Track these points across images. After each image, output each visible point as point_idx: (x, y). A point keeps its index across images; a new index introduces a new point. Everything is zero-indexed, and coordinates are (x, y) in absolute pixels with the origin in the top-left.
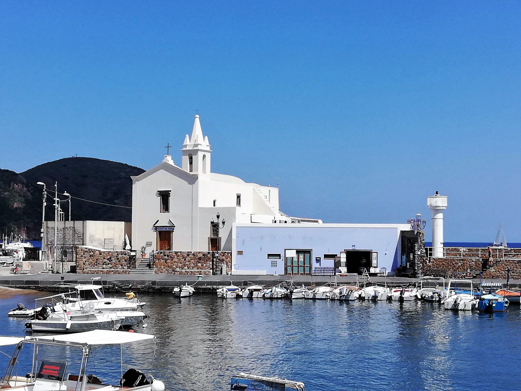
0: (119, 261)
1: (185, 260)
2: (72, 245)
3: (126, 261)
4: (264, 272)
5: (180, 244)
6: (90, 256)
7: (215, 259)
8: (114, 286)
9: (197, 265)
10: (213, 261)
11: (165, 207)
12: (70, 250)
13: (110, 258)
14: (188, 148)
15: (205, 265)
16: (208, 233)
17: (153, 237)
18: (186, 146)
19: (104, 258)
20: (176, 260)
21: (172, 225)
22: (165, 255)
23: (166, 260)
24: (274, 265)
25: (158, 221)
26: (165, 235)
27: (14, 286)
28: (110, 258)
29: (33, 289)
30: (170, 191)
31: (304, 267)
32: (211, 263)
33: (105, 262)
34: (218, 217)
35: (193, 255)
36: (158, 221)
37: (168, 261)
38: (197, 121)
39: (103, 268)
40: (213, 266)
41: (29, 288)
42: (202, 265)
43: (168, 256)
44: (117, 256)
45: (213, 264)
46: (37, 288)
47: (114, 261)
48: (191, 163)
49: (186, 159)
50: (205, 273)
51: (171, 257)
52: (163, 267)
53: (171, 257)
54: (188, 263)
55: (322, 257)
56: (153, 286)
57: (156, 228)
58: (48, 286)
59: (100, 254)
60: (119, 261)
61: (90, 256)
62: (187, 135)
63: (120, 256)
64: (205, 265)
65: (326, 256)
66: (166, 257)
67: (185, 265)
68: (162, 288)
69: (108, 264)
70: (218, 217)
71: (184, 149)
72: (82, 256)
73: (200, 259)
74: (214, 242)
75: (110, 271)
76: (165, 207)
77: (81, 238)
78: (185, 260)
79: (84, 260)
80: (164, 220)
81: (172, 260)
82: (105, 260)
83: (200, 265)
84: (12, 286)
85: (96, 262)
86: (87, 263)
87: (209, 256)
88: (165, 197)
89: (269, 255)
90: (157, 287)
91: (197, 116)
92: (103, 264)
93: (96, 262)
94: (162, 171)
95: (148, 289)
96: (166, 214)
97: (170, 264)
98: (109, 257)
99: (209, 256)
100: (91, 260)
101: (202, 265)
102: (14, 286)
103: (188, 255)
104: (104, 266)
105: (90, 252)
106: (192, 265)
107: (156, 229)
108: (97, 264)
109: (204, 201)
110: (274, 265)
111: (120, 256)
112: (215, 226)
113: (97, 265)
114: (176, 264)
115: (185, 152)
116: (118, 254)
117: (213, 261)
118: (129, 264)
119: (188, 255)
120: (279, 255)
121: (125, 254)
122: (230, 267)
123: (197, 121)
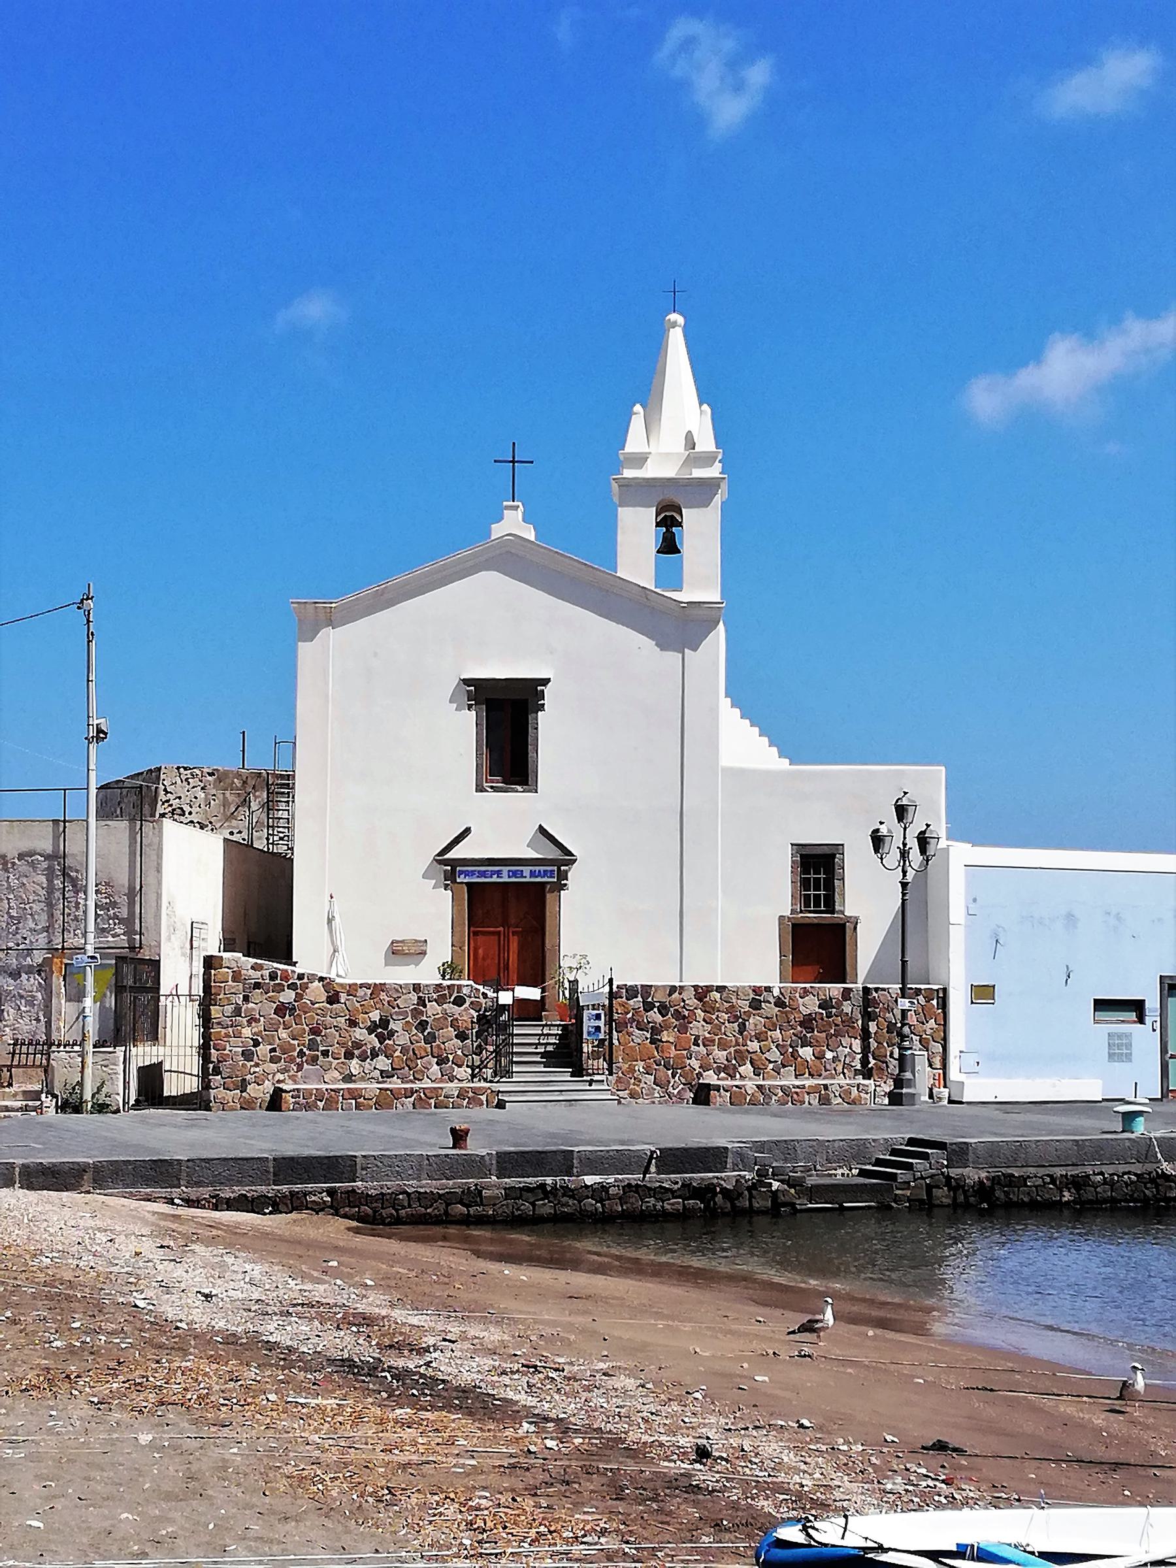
0: (430, 1039)
1: (742, 1028)
2: (38, 957)
3: (462, 1036)
4: (1090, 1089)
5: (598, 944)
6: (281, 1010)
7: (873, 1027)
8: (762, 1174)
9: (795, 1055)
10: (865, 1035)
12: (30, 983)
13: (384, 1023)
14: (651, 471)
15: (829, 1055)
16: (778, 897)
17: (435, 918)
18: (640, 460)
19: (353, 1023)
20: (699, 1028)
21: (554, 853)
22: (648, 1007)
23: (656, 1031)
24: (1119, 1051)
25: (467, 831)
26: (508, 912)
27: (205, 1192)
28: (384, 1023)
29: (318, 1208)
30: (545, 682)
32: (857, 1045)
33: (358, 1045)
34: (901, 811)
35: (779, 1003)
36: (467, 831)
37: (665, 1036)
38: (676, 341)
39: (349, 1078)
40: (865, 1062)
41: (295, 1203)
42: (820, 1057)
44: (416, 1013)
45: (866, 1049)
47: (402, 1039)
48: (669, 546)
49: (637, 528)
50: (845, 1095)
51: (678, 1015)
53: (678, 1015)
54: (754, 1046)
56: (954, 1172)
57: (449, 868)
58: (412, 1185)
59: (333, 999)
60: (430, 1039)
61: (281, 1010)
62: (638, 408)
63: (433, 1009)
64: (829, 1055)
66: (655, 1016)
67: (741, 1056)
68: (994, 1180)
69: (375, 1054)
71: (628, 473)
72: (237, 1012)
73: (808, 1022)
74: (818, 943)
75: (395, 1094)
77: (124, 913)
78: (742, 1028)
79: (247, 1032)
80: (502, 829)
81: (683, 1029)
82: (360, 1034)
83: (806, 1052)
84: (192, 1192)
85: (312, 1045)
86: (263, 1049)
87: (847, 1007)
89: (1101, 1005)
90: (973, 1174)
91: (674, 317)
92: (349, 1055)
93: (312, 1045)
94: (490, 579)
95: (929, 1188)
96: (517, 798)
97: (673, 1052)
98: (375, 1016)
99: (847, 1007)
100: (283, 1034)
101: (820, 1057)
102: (205, 1192)
103: (756, 1005)
104: (354, 1066)
105: (279, 989)
106: (775, 1055)
107: (451, 877)
108: (313, 1052)
110: (1119, 1051)
111: (433, 1009)
113: (314, 1060)
114: (702, 1049)
115: (637, 491)
116: (422, 1002)
117: (865, 1035)
118: (479, 1051)
120: (1137, 1007)
121: (459, 1002)
122: (937, 1062)
123: (676, 341)
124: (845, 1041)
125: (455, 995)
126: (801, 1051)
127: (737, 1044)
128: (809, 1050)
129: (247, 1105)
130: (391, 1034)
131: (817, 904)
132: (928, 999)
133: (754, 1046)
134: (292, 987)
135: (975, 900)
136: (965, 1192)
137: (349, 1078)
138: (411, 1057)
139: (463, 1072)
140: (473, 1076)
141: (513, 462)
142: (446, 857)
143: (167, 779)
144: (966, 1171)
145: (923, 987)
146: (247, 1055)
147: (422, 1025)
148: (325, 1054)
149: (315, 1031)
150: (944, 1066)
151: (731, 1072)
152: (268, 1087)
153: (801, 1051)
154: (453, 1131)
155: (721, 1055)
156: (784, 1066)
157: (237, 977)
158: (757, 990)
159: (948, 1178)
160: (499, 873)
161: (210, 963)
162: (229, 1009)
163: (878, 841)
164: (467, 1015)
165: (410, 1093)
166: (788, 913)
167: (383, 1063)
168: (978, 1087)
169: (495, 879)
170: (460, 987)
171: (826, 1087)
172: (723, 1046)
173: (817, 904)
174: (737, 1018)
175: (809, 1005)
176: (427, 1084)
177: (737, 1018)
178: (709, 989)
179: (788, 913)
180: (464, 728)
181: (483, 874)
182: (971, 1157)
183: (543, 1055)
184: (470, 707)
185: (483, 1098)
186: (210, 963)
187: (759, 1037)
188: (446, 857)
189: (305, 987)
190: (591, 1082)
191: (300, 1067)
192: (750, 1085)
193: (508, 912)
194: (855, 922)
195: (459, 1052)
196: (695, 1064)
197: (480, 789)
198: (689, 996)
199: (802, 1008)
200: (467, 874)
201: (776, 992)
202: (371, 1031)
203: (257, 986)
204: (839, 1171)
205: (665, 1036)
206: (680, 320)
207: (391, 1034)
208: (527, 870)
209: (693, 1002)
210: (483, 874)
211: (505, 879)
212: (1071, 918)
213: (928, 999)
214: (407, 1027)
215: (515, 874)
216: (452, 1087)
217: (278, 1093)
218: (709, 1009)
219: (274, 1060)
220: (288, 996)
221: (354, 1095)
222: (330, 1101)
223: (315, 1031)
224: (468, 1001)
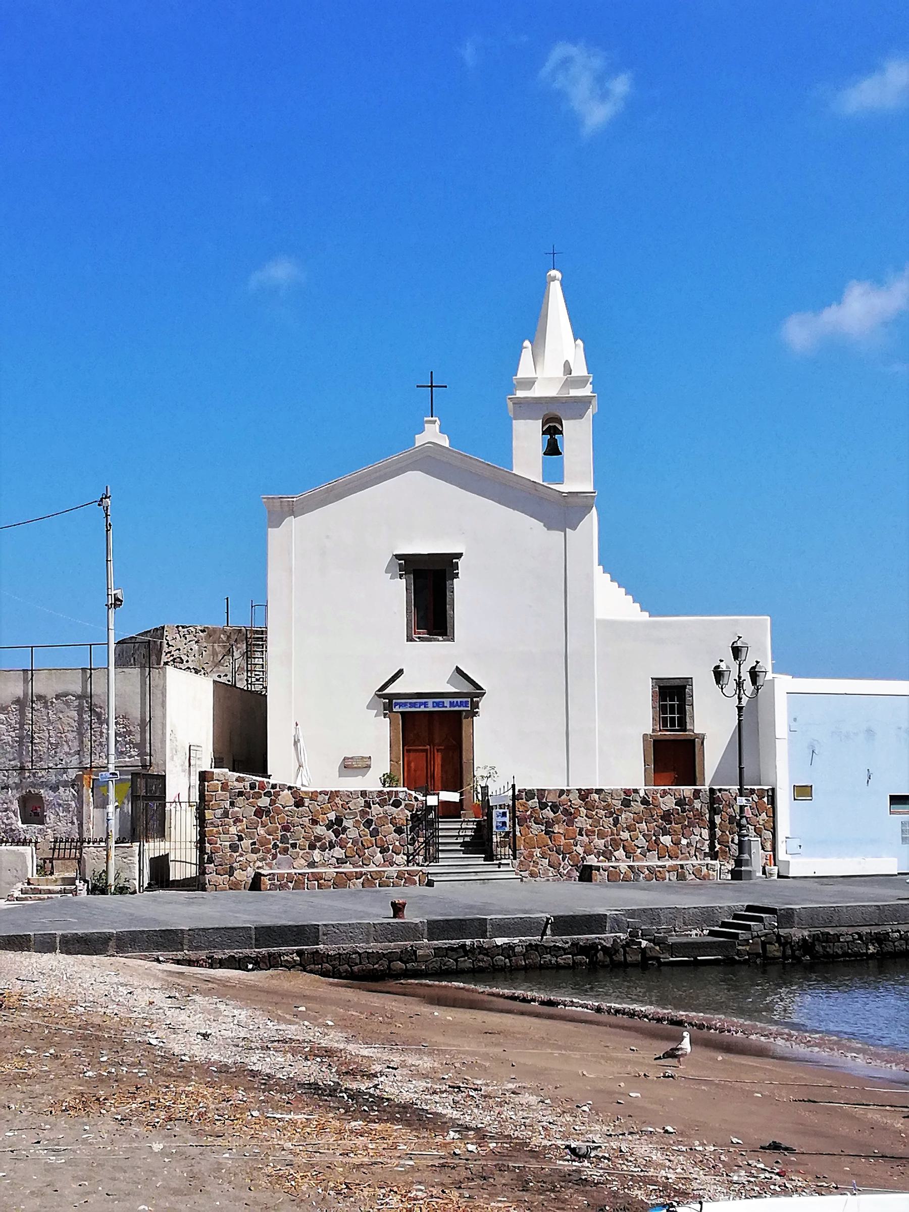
1: (616, 822)
2: (72, 774)
3: (399, 831)
5: (503, 758)
6: (259, 812)
7: (718, 820)
8: (633, 935)
9: (657, 842)
10: (712, 826)
12: (66, 794)
13: (339, 821)
14: (537, 392)
15: (684, 842)
16: (642, 719)
17: (376, 739)
18: (529, 383)
19: (315, 822)
20: (582, 822)
21: (467, 688)
22: (543, 806)
23: (549, 824)
25: (400, 672)
26: (433, 734)
27: (203, 954)
28: (339, 821)
29: (290, 966)
30: (459, 556)
32: (705, 833)
33: (318, 838)
34: (736, 652)
35: (645, 802)
36: (400, 672)
37: (556, 829)
38: (556, 292)
39: (312, 864)
40: (712, 846)
41: (271, 962)
42: (677, 843)
43: (555, 808)
44: (363, 813)
45: (712, 836)
46: (312, 963)
47: (353, 833)
48: (553, 449)
49: (528, 436)
50: (697, 873)
51: (566, 812)
52: (537, 852)
53: (566, 812)
54: (625, 835)
56: (782, 932)
57: (387, 701)
58: (361, 947)
59: (299, 803)
61: (259, 812)
62: (527, 343)
63: (376, 809)
64: (684, 842)
66: (548, 813)
67: (616, 844)
68: (815, 937)
69: (332, 846)
71: (520, 394)
72: (226, 814)
73: (667, 816)
74: (674, 755)
75: (348, 877)
77: (137, 739)
78: (616, 822)
79: (233, 830)
80: (428, 670)
81: (570, 823)
82: (320, 830)
83: (666, 840)
84: (192, 955)
85: (284, 839)
86: (246, 843)
90: (798, 933)
91: (554, 273)
92: (312, 847)
93: (284, 839)
94: (415, 477)
95: (764, 944)
96: (438, 647)
97: (563, 841)
98: (332, 816)
99: (697, 804)
100: (261, 831)
101: (677, 843)
102: (203, 954)
103: (626, 803)
104: (317, 855)
106: (642, 842)
107: (388, 707)
108: (284, 845)
113: (286, 851)
114: (585, 838)
116: (368, 805)
117: (712, 826)
119: (626, 803)
121: (397, 804)
123: (556, 292)
124: (697, 831)
125: (393, 799)
126: (662, 839)
127: (612, 834)
128: (668, 838)
129: (234, 886)
130: (345, 830)
131: (673, 725)
132: (761, 797)
133: (625, 835)
134: (268, 794)
135: (795, 720)
136: (792, 947)
137: (312, 864)
138: (360, 848)
139: (401, 859)
140: (408, 861)
141: (432, 386)
142: (385, 692)
143: (169, 635)
144: (793, 931)
145: (756, 787)
146: (234, 848)
147: (369, 823)
148: (294, 846)
150: (774, 849)
151: (608, 856)
152: (251, 872)
153: (662, 839)
154: (394, 904)
155: (600, 843)
156: (649, 851)
157: (225, 787)
158: (627, 792)
159: (779, 936)
160: (425, 704)
161: (204, 777)
162: (219, 812)
163: (719, 675)
164: (402, 814)
165: (359, 876)
166: (650, 732)
167: (338, 852)
168: (800, 865)
169: (422, 709)
170: (397, 792)
171: (682, 866)
172: (601, 836)
173: (673, 725)
174: (611, 814)
175: (668, 804)
176: (372, 868)
177: (611, 814)
178: (589, 792)
179: (650, 732)
180: (397, 592)
181: (413, 705)
182: (796, 919)
183: (462, 844)
184: (401, 576)
185: (417, 878)
186: (204, 777)
187: (629, 829)
188: (385, 692)
189: (277, 794)
190: (499, 865)
191: (274, 857)
192: (623, 866)
193: (433, 734)
194: (702, 738)
195: (397, 843)
196: (580, 850)
197: (410, 639)
198: (574, 797)
199: (662, 806)
200: (401, 705)
201: (642, 793)
203: (241, 794)
204: (694, 932)
205: (556, 829)
206: (558, 275)
207: (345, 830)
208: (447, 701)
209: (578, 802)
210: (413, 705)
211: (431, 709)
212: (870, 732)
213: (761, 797)
214: (356, 825)
215: (438, 704)
216: (392, 870)
217: (258, 877)
218: (590, 807)
220: (264, 802)
221: (317, 877)
222: (298, 883)
223: (286, 829)
224: (403, 803)
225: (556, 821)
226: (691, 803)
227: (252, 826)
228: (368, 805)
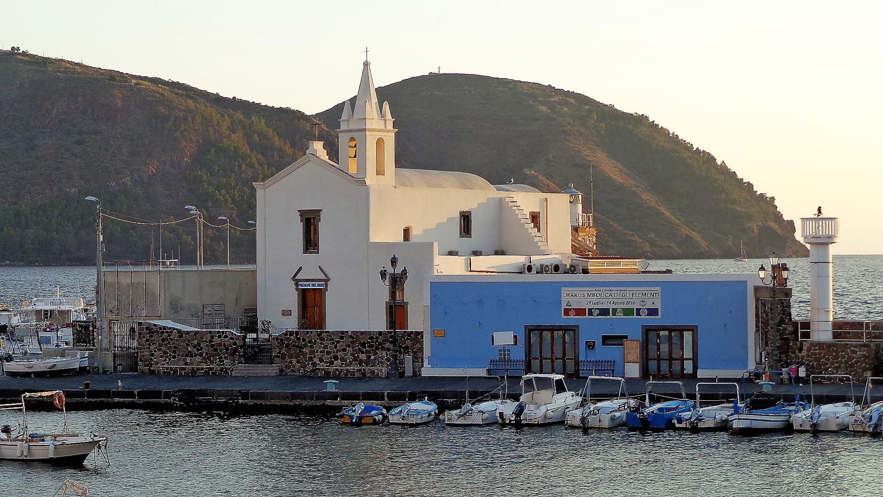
0: (215, 350)
6: (163, 340)
11: (311, 243)
15: (372, 358)
17: (292, 302)
19: (188, 345)
21: (324, 278)
23: (301, 348)
25: (300, 269)
28: (199, 345)
31: (563, 359)
33: (189, 352)
34: (394, 262)
36: (300, 269)
39: (186, 364)
44: (211, 341)
55: (599, 342)
61: (163, 340)
63: (216, 340)
65: (606, 340)
67: (336, 358)
69: (196, 356)
70: (394, 262)
76: (311, 243)
80: (311, 267)
81: (312, 347)
83: (363, 357)
88: (310, 222)
92: (187, 356)
98: (195, 342)
100: (164, 348)
104: (188, 360)
105: (162, 333)
109: (385, 231)
112: (397, 282)
113: (174, 357)
116: (212, 337)
149: (175, 347)
155: (326, 358)
163: (383, 274)
168: (427, 371)
193: (311, 301)
202: (194, 347)
208: (317, 283)
219: (162, 357)
225: (305, 346)
226: (377, 338)
227: (160, 345)
228: (212, 337)
